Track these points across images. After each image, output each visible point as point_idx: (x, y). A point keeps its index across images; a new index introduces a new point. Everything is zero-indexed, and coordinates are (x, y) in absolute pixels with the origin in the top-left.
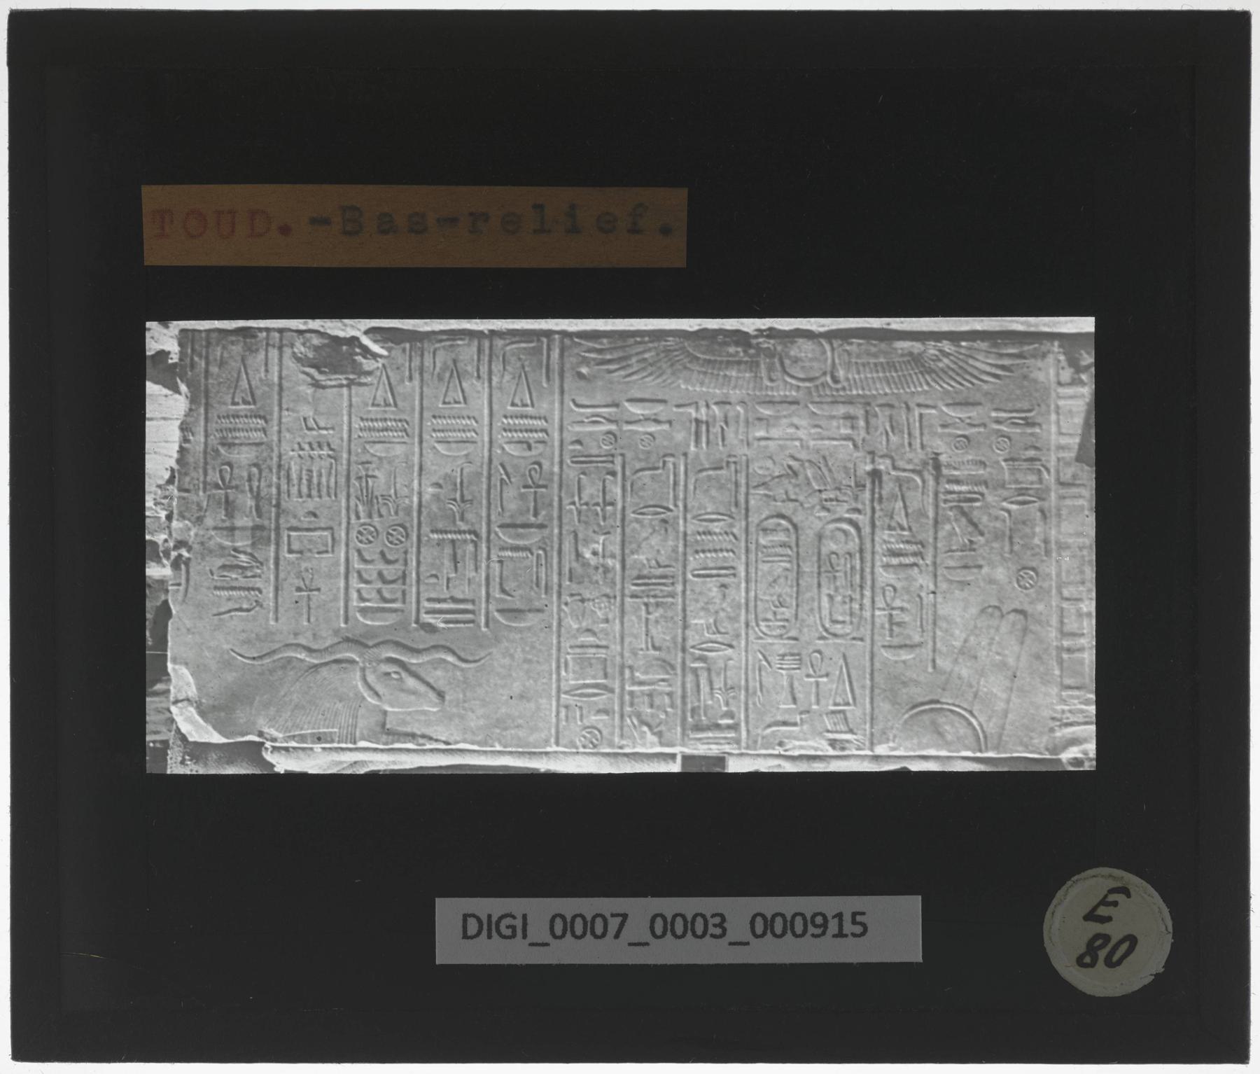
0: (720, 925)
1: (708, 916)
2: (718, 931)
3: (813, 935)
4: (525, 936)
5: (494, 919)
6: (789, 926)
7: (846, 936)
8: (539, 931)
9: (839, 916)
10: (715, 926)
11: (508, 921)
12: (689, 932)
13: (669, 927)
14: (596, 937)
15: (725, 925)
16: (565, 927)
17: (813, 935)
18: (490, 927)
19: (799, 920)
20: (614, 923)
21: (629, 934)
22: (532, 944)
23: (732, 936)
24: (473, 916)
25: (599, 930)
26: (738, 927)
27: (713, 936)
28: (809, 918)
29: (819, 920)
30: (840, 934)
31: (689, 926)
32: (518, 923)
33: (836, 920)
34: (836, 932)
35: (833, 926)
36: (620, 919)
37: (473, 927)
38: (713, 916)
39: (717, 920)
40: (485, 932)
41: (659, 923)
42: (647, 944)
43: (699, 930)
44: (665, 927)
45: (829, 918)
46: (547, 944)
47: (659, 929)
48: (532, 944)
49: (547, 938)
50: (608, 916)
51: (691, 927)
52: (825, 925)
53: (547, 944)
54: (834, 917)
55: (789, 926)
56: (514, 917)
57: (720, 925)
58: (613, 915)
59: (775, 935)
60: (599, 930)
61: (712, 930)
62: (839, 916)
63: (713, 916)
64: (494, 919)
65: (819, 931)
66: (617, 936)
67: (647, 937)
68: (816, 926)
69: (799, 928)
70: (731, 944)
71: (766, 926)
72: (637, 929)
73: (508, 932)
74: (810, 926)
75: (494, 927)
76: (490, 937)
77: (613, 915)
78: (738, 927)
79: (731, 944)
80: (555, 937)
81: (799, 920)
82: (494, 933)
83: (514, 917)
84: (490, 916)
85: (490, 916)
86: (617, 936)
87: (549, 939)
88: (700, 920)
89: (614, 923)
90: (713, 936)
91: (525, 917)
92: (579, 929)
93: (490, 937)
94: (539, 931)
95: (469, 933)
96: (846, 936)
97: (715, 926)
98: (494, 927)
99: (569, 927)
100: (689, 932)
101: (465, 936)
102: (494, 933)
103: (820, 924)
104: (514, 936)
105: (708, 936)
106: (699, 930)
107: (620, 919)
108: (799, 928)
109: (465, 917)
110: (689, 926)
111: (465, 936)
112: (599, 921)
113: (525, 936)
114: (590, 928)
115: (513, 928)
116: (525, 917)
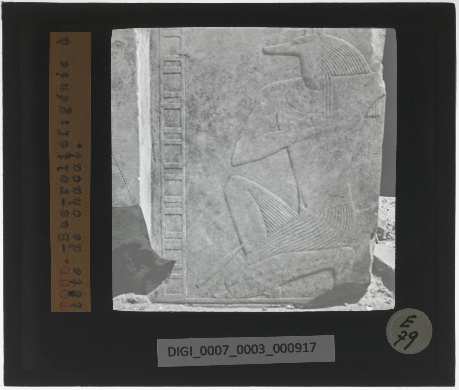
0: (262, 349)
1: (258, 346)
2: (261, 351)
3: (296, 352)
4: (191, 355)
5: (180, 349)
6: (287, 348)
7: (308, 351)
8: (196, 352)
9: (306, 344)
10: (260, 349)
11: (185, 349)
12: (251, 351)
13: (244, 349)
14: (218, 354)
15: (264, 348)
16: (205, 351)
17: (296, 352)
18: (179, 351)
19: (291, 346)
20: (224, 349)
21: (229, 353)
22: (194, 358)
23: (266, 353)
24: (172, 348)
25: (218, 352)
26: (269, 349)
27: (260, 353)
28: (295, 346)
29: (298, 346)
30: (306, 351)
31: (251, 349)
32: (189, 350)
33: (305, 346)
34: (305, 350)
35: (303, 348)
36: (226, 347)
37: (172, 352)
38: (260, 345)
39: (261, 347)
40: (177, 354)
41: (240, 349)
42: (236, 356)
43: (255, 351)
44: (242, 350)
45: (302, 345)
46: (200, 357)
47: (240, 351)
48: (194, 358)
49: (199, 355)
50: (221, 347)
51: (251, 349)
52: (300, 348)
53: (200, 357)
54: (304, 345)
55: (287, 348)
56: (187, 348)
57: (262, 349)
58: (223, 346)
59: (282, 352)
60: (218, 352)
61: (259, 350)
62: (306, 344)
63: (260, 345)
64: (180, 349)
65: (298, 350)
66: (225, 354)
67: (235, 353)
68: (297, 348)
69: (291, 349)
70: (266, 355)
71: (279, 348)
72: (232, 350)
73: (185, 353)
74: (295, 348)
75: (180, 352)
76: (178, 355)
77: (223, 346)
78: (269, 349)
79: (266, 355)
80: (202, 354)
81: (291, 346)
82: (180, 354)
83: (187, 348)
84: (178, 348)
85: (178, 348)
86: (225, 354)
87: (200, 355)
88: (255, 348)
89: (224, 349)
90: (260, 353)
91: (191, 348)
92: (211, 350)
93: (178, 355)
94: (196, 352)
95: (171, 355)
96: (308, 351)
97: (260, 349)
98: (180, 352)
99: (207, 350)
100: (251, 351)
101: (170, 355)
102: (180, 354)
103: (298, 347)
104: (187, 354)
105: (258, 352)
106: (255, 351)
107: (226, 347)
108: (291, 349)
109: (169, 348)
110: (251, 349)
111: (170, 355)
112: (218, 350)
113: (191, 355)
114: (215, 351)
115: (187, 352)
116: (191, 348)
